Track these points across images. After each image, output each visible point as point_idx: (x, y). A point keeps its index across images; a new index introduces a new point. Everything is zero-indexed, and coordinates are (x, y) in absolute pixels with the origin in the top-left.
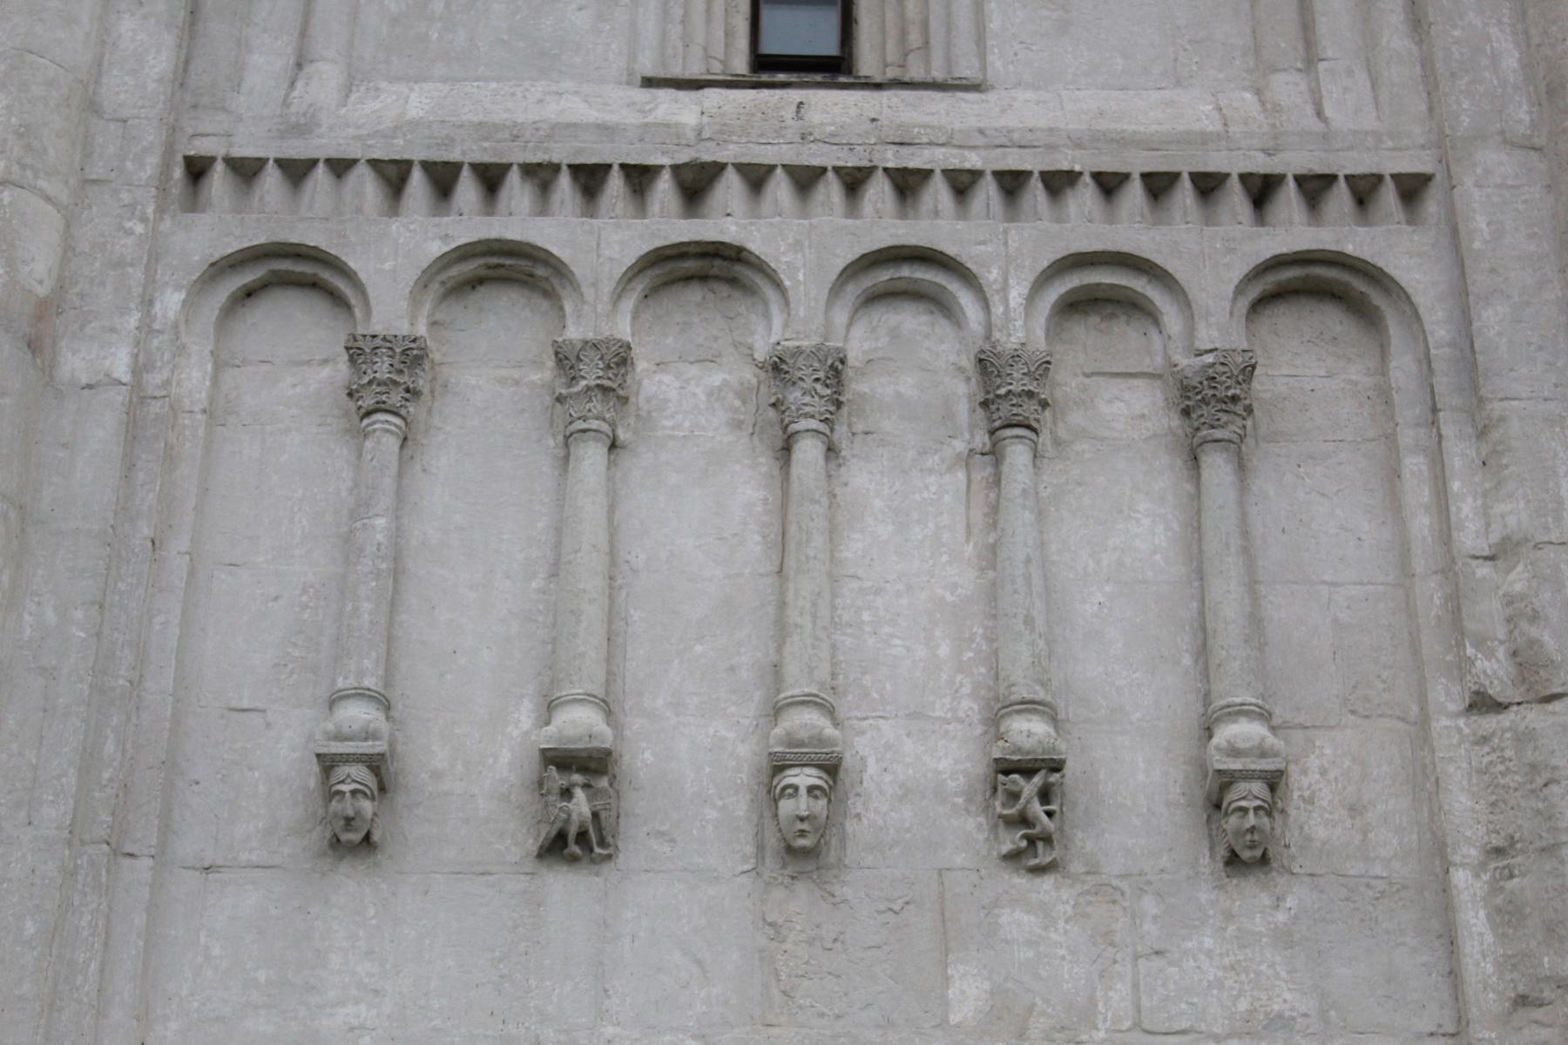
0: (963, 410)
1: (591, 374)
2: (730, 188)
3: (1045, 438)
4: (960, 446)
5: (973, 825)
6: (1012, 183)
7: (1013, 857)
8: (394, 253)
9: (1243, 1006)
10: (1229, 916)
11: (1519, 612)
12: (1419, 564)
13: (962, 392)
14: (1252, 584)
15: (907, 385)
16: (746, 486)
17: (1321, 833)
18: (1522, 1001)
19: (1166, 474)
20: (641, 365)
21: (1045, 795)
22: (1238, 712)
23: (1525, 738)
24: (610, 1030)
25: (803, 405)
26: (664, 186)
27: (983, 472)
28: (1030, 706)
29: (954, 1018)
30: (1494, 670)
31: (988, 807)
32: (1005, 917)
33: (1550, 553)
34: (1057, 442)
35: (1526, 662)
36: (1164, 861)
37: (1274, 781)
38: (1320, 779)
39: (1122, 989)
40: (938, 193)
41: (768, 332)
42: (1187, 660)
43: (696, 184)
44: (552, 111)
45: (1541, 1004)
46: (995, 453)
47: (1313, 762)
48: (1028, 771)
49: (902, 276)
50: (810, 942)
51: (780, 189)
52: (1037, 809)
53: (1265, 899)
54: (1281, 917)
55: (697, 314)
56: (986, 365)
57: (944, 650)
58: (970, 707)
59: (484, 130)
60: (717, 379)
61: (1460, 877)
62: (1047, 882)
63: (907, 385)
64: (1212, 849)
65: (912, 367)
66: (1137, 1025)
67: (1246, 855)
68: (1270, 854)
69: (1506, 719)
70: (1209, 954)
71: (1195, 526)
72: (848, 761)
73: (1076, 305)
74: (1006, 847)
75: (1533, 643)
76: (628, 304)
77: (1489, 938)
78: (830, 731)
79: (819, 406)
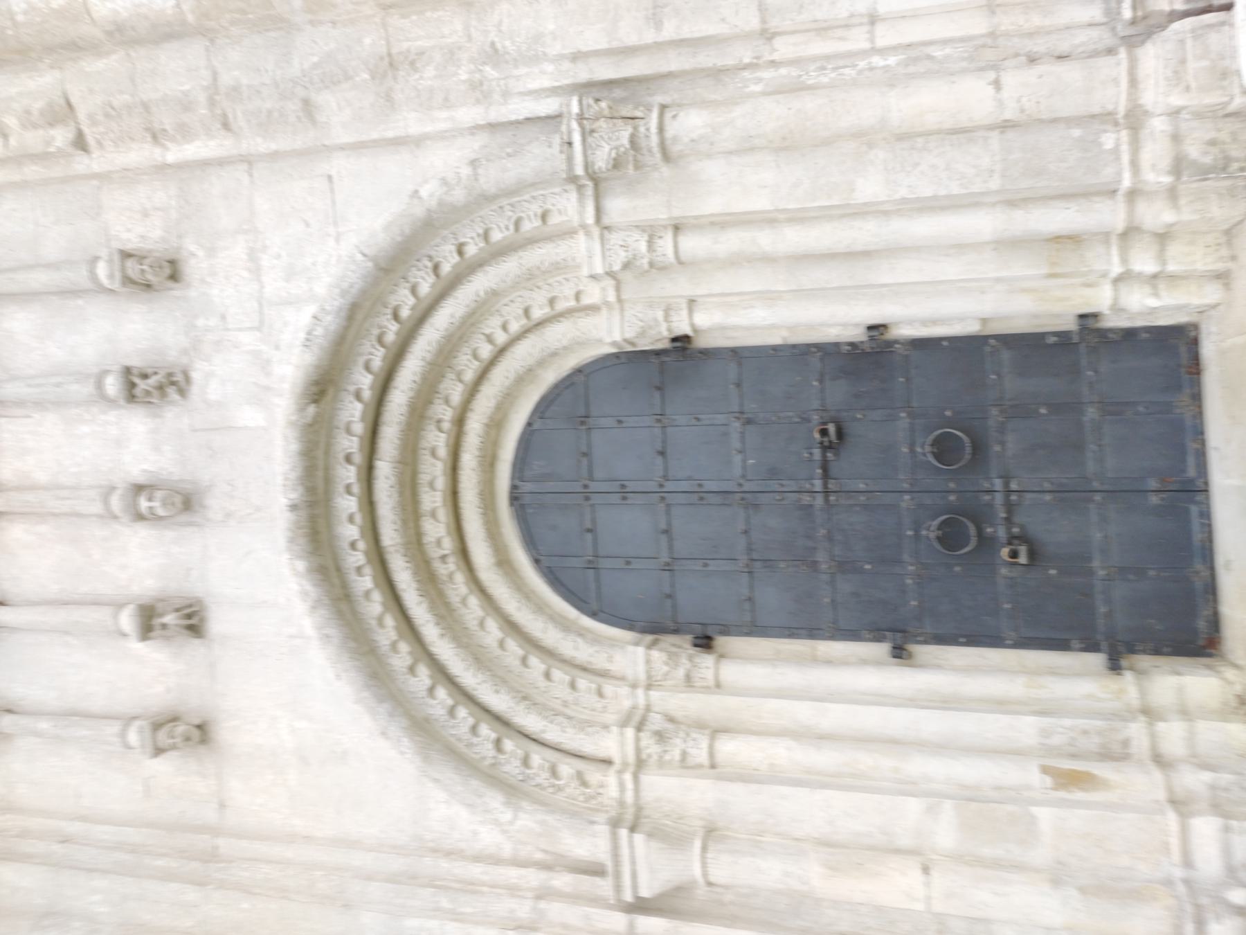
7: (182, 392)
9: (245, 274)
10: (203, 281)
18: (226, 126)
21: (145, 376)
38: (131, 234)
45: (225, 115)
47: (125, 236)
48: (133, 385)
52: (152, 381)
53: (193, 262)
54: (201, 253)
58: (112, 416)
62: (195, 375)
64: (171, 289)
66: (259, 329)
67: (168, 271)
68: (168, 258)
77: (198, 143)
78: (119, 492)
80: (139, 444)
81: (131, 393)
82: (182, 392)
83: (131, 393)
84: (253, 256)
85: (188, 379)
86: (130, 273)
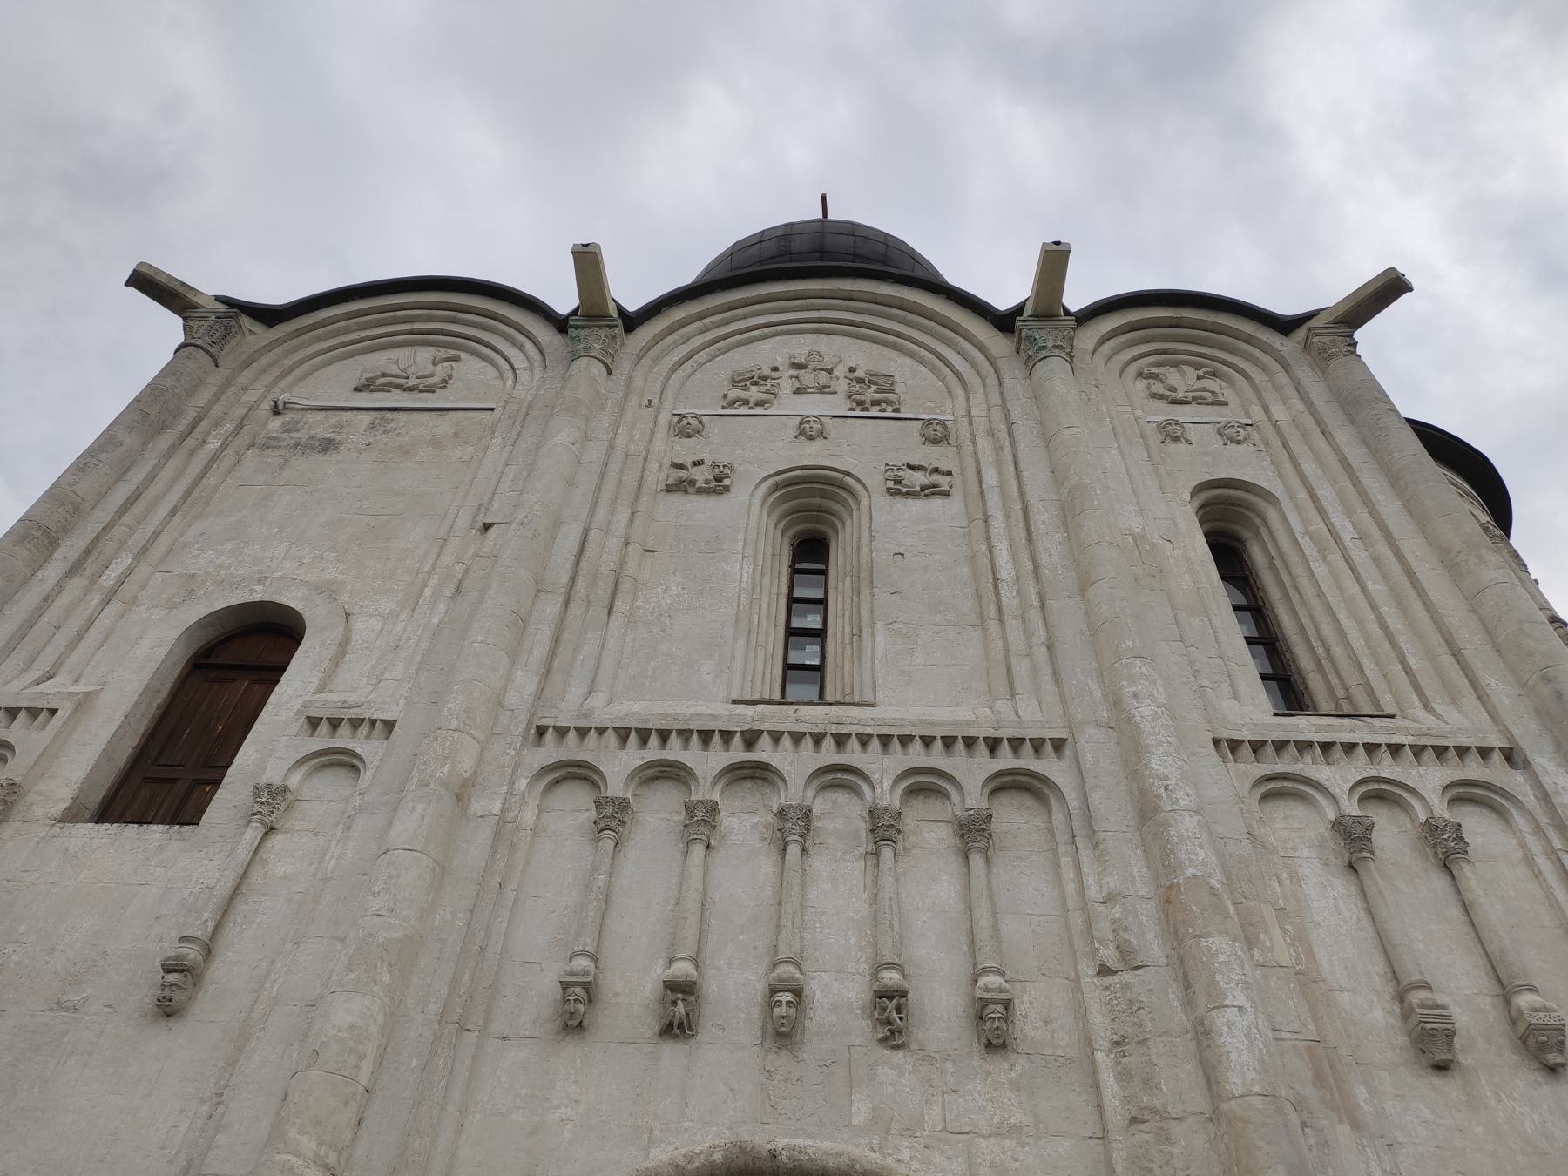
0: (863, 834)
1: (699, 815)
2: (765, 741)
3: (899, 847)
4: (862, 850)
5: (865, 1025)
6: (885, 740)
7: (884, 1040)
8: (618, 766)
9: (996, 1120)
11: (1118, 927)
12: (1070, 906)
13: (863, 827)
14: (994, 913)
15: (839, 823)
16: (766, 865)
17: (1031, 1033)
18: (1134, 1120)
19: (953, 864)
20: (723, 814)
21: (898, 1009)
22: (990, 971)
23: (1126, 987)
24: (687, 1124)
25: (793, 830)
26: (737, 739)
27: (871, 861)
28: (891, 966)
29: (855, 1122)
30: (1109, 955)
31: (872, 1015)
32: (880, 1070)
33: (1131, 900)
34: (905, 849)
35: (1124, 951)
36: (956, 1045)
37: (1007, 1004)
39: (937, 1109)
40: (854, 743)
41: (778, 800)
42: (965, 948)
43: (751, 739)
44: (692, 710)
46: (877, 853)
47: (1026, 998)
48: (891, 998)
49: (837, 778)
50: (786, 1081)
51: (786, 741)
53: (1006, 1066)
55: (748, 794)
56: (873, 813)
57: (853, 941)
58: (864, 967)
59: (663, 716)
60: (755, 820)
61: (1100, 1056)
62: (901, 1053)
63: (839, 823)
65: (840, 817)
66: (944, 1128)
67: (995, 1042)
69: (1116, 978)
70: (979, 1092)
71: (967, 887)
72: (807, 991)
73: (914, 791)
74: (880, 1036)
75: (1126, 941)
76: (719, 787)
77: (1116, 1087)
79: (798, 830)
80: (838, 992)
81: (883, 995)
82: (884, 1040)
83: (883, 995)
84: (1014, 1130)
85: (896, 1048)
86: (992, 1007)
